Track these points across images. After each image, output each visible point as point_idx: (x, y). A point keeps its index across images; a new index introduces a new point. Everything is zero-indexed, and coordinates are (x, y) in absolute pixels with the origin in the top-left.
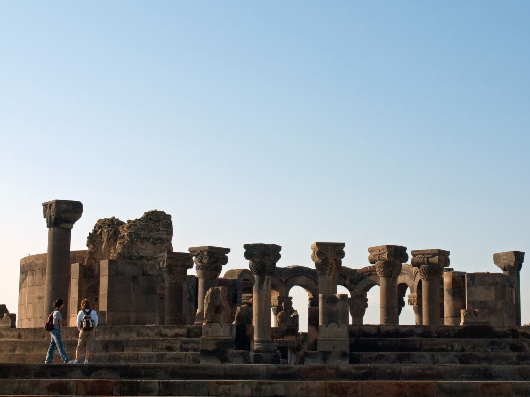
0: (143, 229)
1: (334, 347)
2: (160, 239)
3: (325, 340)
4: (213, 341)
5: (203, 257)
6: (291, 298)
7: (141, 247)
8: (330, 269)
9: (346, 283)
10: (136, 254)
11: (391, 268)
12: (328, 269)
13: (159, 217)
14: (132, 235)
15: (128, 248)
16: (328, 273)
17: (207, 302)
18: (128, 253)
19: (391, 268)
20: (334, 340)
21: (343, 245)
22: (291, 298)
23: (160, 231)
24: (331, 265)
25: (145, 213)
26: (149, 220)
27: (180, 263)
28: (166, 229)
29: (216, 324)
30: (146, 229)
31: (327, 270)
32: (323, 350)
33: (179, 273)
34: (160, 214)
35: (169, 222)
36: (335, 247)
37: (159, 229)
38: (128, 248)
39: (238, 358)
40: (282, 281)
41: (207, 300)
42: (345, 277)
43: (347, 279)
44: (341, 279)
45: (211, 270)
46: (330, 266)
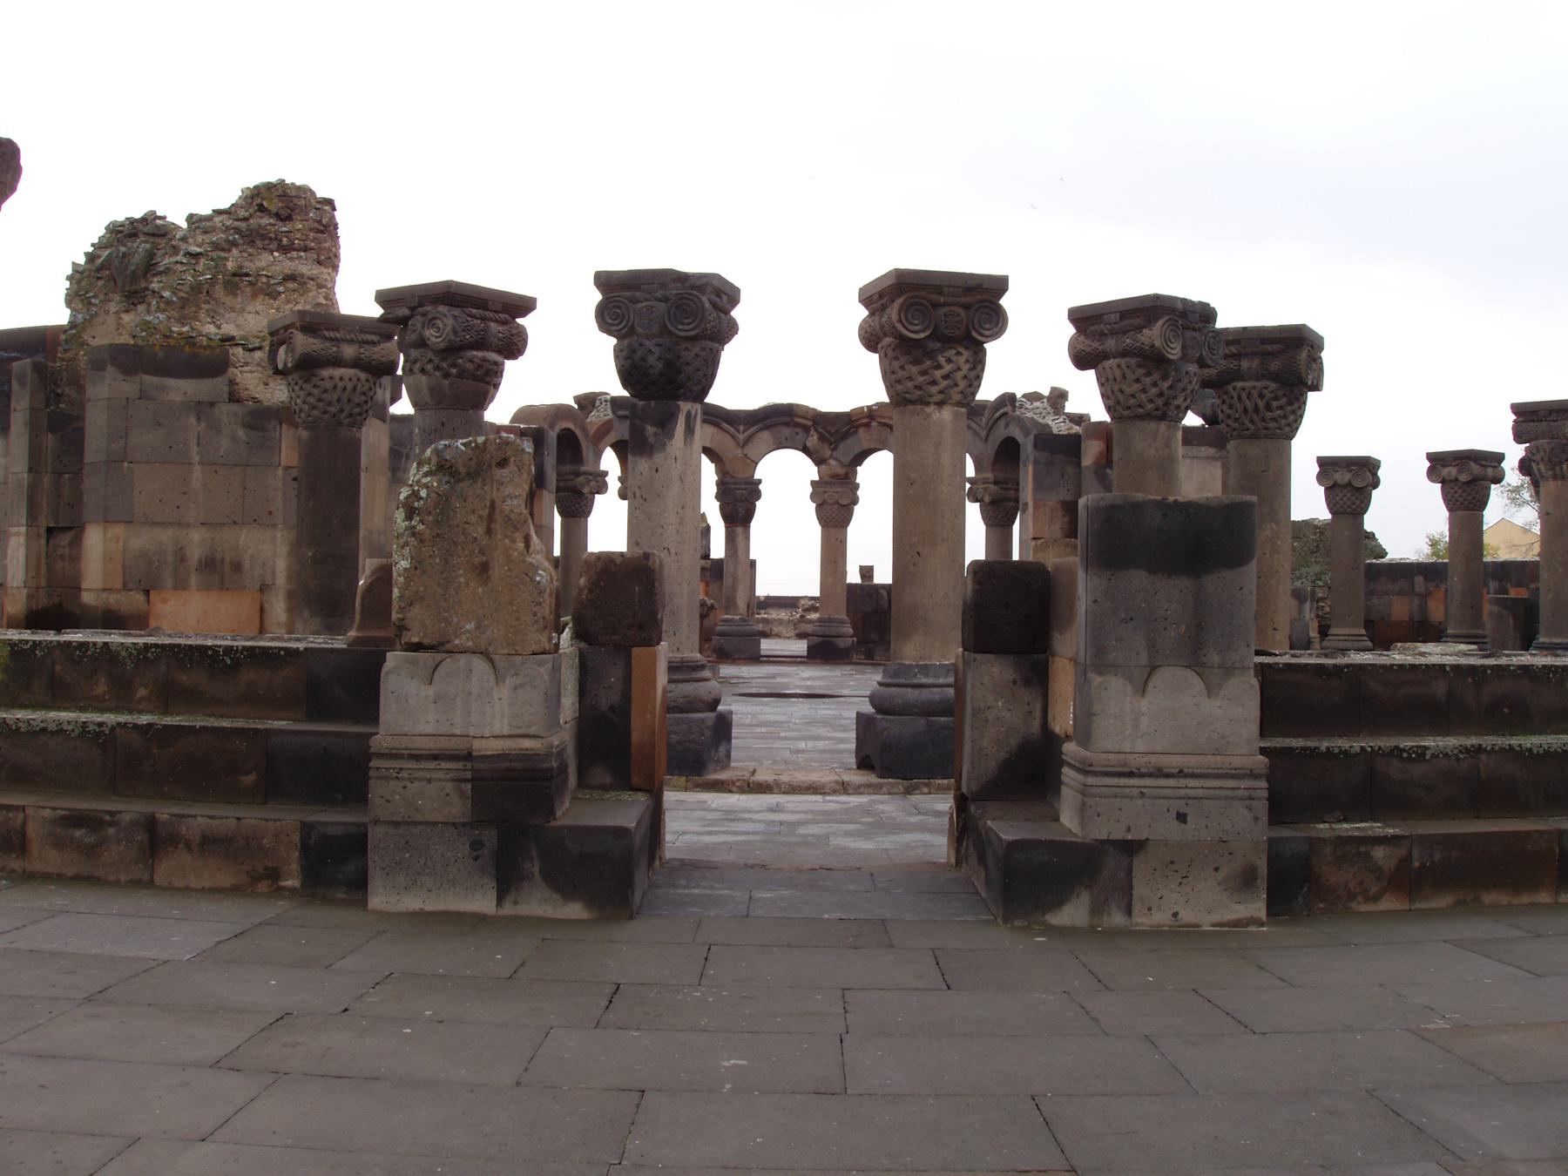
0: (234, 244)
1: (1182, 818)
2: (291, 277)
3: (1130, 775)
4: (444, 765)
9: (808, 444)
10: (211, 329)
11: (1165, 385)
12: (938, 378)
13: (292, 202)
14: (197, 263)
19: (1165, 385)
20: (1181, 771)
23: (294, 250)
26: (259, 214)
31: (934, 383)
33: (345, 389)
38: (183, 308)
41: (409, 517)
42: (806, 429)
46: (948, 368)
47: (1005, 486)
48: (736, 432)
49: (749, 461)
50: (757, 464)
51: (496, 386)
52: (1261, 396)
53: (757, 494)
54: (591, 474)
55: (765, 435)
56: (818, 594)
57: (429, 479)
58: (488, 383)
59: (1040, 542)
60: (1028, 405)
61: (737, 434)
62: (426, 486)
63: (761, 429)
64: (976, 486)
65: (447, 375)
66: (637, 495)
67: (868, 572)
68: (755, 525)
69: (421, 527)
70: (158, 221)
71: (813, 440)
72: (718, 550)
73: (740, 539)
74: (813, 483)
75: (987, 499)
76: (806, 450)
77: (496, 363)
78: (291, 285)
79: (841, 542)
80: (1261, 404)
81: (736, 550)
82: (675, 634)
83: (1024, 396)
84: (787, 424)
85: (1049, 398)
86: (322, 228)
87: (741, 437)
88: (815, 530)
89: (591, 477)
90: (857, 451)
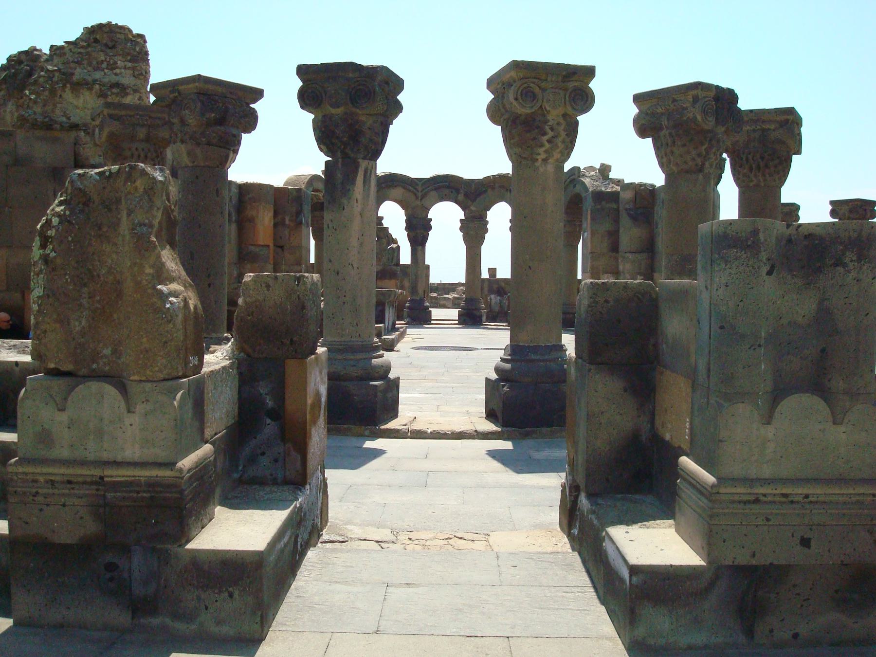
1: (805, 542)
2: (117, 85)
3: (757, 501)
5: (185, 105)
7: (75, 102)
8: (549, 141)
10: (64, 119)
15: (44, 106)
16: (542, 153)
17: (45, 259)
18: (45, 117)
21: (589, 72)
23: (117, 68)
24: (552, 129)
25: (86, 29)
26: (94, 44)
27: (142, 133)
28: (129, 65)
29: (94, 386)
30: (85, 62)
31: (542, 146)
32: (743, 559)
34: (117, 30)
35: (137, 49)
36: (565, 77)
37: (116, 63)
38: (44, 106)
39: (231, 595)
41: (43, 246)
42: (458, 191)
44: (452, 192)
45: (209, 144)
46: (551, 134)
50: (428, 210)
51: (236, 152)
52: (762, 158)
53: (429, 228)
55: (433, 193)
57: (62, 207)
58: (230, 149)
60: (587, 174)
61: (417, 192)
62: (58, 215)
63: (432, 190)
65: (198, 144)
66: (329, 226)
68: (429, 245)
69: (53, 254)
70: (35, 52)
71: (461, 197)
72: (405, 258)
73: (419, 253)
74: (461, 220)
76: (457, 202)
77: (234, 136)
78: (114, 90)
80: (762, 164)
82: (357, 325)
83: (584, 169)
84: (448, 187)
85: (599, 169)
86: (135, 53)
87: (420, 194)
88: (462, 248)
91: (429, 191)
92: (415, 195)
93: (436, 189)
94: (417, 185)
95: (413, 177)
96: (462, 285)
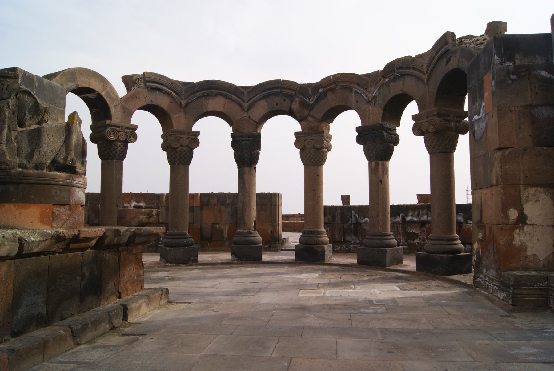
6: (198, 133)
9: (293, 107)
22: (198, 133)
40: (181, 104)
42: (291, 98)
43: (296, 101)
44: (284, 100)
47: (446, 118)
48: (242, 102)
49: (252, 121)
54: (119, 127)
55: (263, 103)
56: (303, 212)
59: (507, 152)
63: (261, 99)
64: (419, 122)
67: (347, 199)
74: (296, 134)
75: (431, 130)
79: (318, 175)
81: (244, 184)
87: (246, 105)
88: (300, 168)
89: (118, 129)
90: (327, 108)
91: (256, 101)
92: (240, 105)
93: (264, 97)
94: (243, 93)
95: (237, 85)
96: (300, 215)
